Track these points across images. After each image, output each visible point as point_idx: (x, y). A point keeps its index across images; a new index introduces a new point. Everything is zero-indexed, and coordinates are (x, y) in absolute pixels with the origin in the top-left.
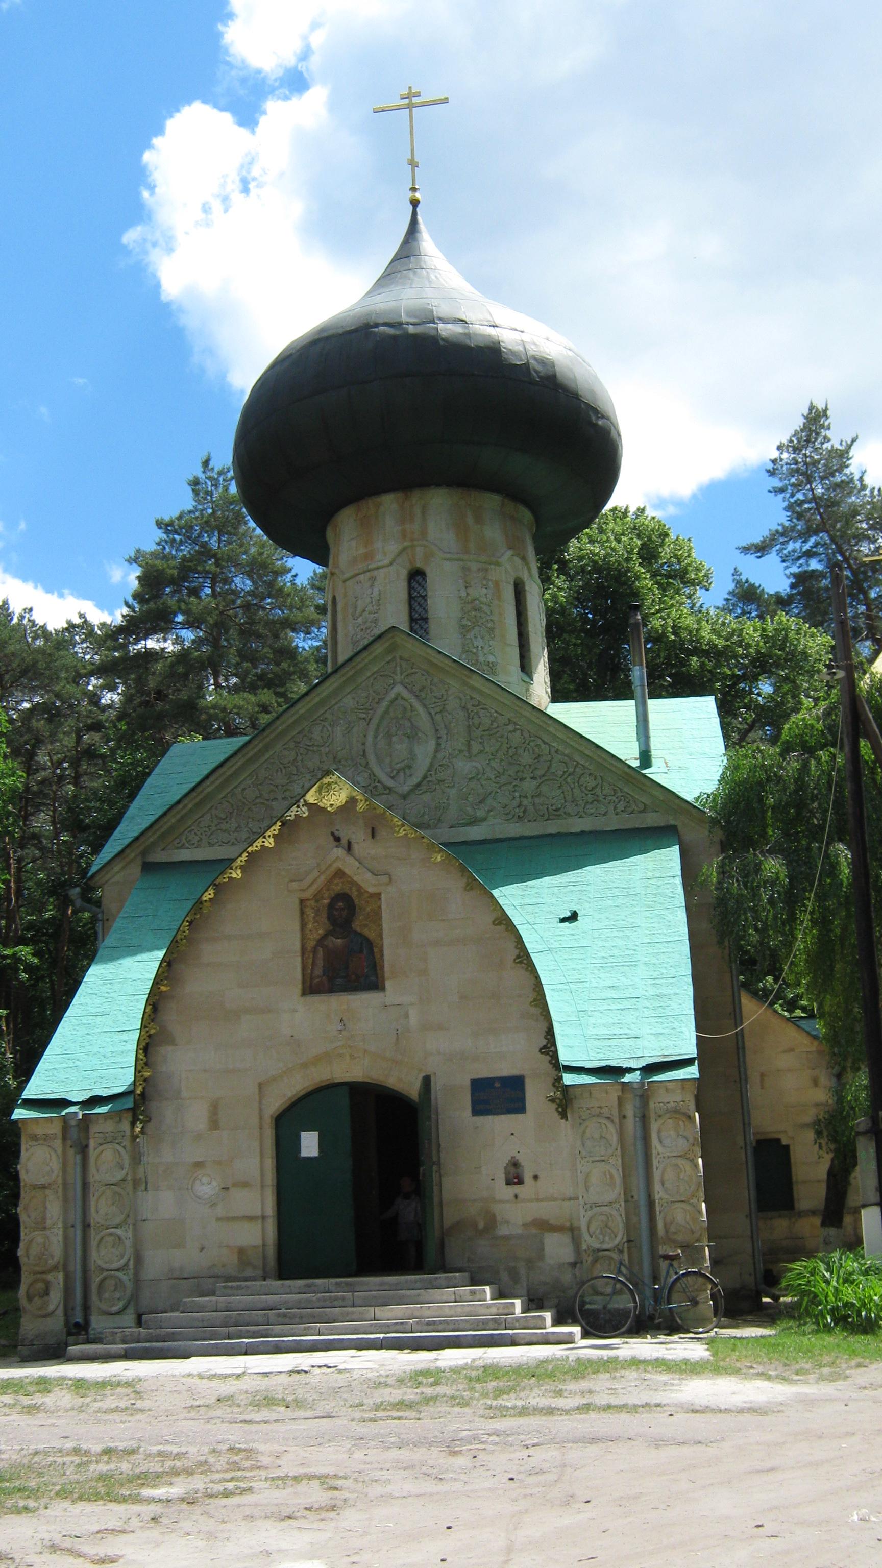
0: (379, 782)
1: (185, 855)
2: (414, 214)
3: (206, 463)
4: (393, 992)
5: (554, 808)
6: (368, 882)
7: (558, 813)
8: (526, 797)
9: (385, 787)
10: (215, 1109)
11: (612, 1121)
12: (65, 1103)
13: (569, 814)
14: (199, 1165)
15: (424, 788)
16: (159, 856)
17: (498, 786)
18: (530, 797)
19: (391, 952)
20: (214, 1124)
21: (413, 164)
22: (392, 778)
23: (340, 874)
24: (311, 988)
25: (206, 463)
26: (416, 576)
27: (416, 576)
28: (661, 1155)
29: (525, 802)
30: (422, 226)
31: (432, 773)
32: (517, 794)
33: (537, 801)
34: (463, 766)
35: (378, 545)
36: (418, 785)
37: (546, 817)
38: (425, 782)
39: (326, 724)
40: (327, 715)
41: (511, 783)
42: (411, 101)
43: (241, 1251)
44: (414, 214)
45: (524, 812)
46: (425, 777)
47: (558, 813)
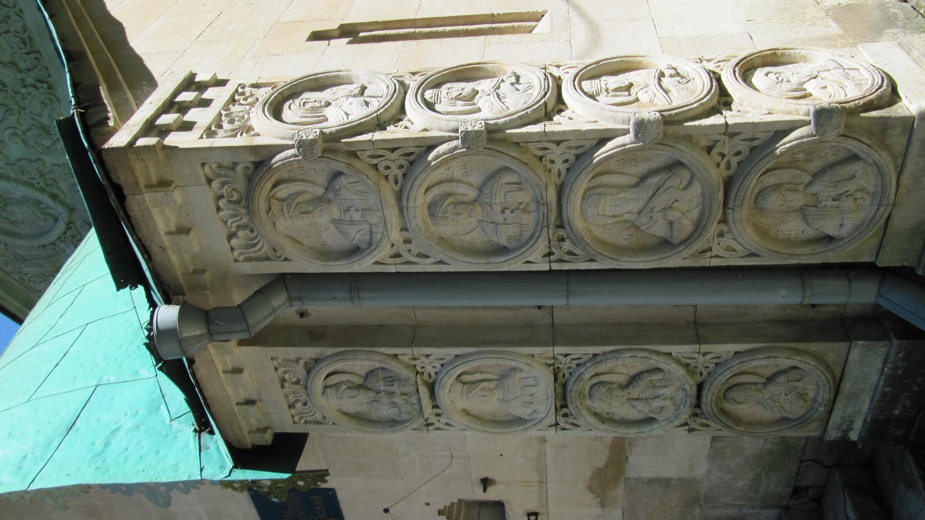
0: (65, 233)
5: (22, 46)
7: (27, 40)
8: (22, 80)
9: (68, 228)
11: (317, 361)
13: (24, 27)
15: (55, 191)
17: (22, 112)
18: (20, 76)
22: (56, 220)
28: (402, 249)
29: (30, 80)
31: (35, 182)
32: (23, 91)
33: (22, 66)
36: (54, 197)
37: (37, 55)
38: (48, 189)
39: (26, 278)
40: (17, 276)
41: (13, 98)
45: (41, 82)
46: (42, 190)
47: (27, 40)
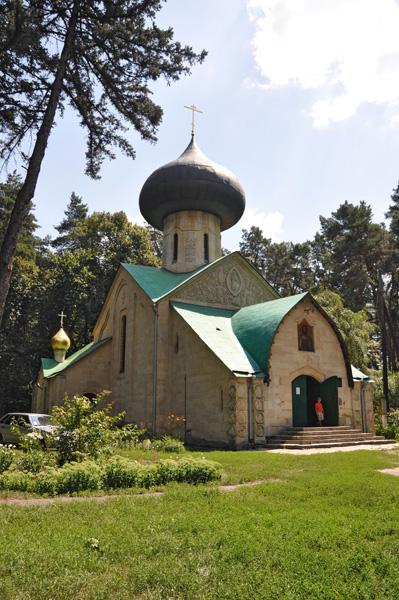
1: (180, 300)
2: (192, 141)
3: (15, 172)
4: (317, 353)
6: (310, 323)
10: (281, 379)
12: (247, 373)
14: (277, 394)
16: (173, 299)
19: (316, 343)
20: (280, 384)
21: (193, 124)
23: (304, 320)
24: (300, 349)
25: (15, 172)
26: (206, 236)
27: (206, 236)
30: (195, 143)
34: (247, 292)
35: (196, 224)
42: (193, 108)
43: (287, 419)
44: (192, 141)
